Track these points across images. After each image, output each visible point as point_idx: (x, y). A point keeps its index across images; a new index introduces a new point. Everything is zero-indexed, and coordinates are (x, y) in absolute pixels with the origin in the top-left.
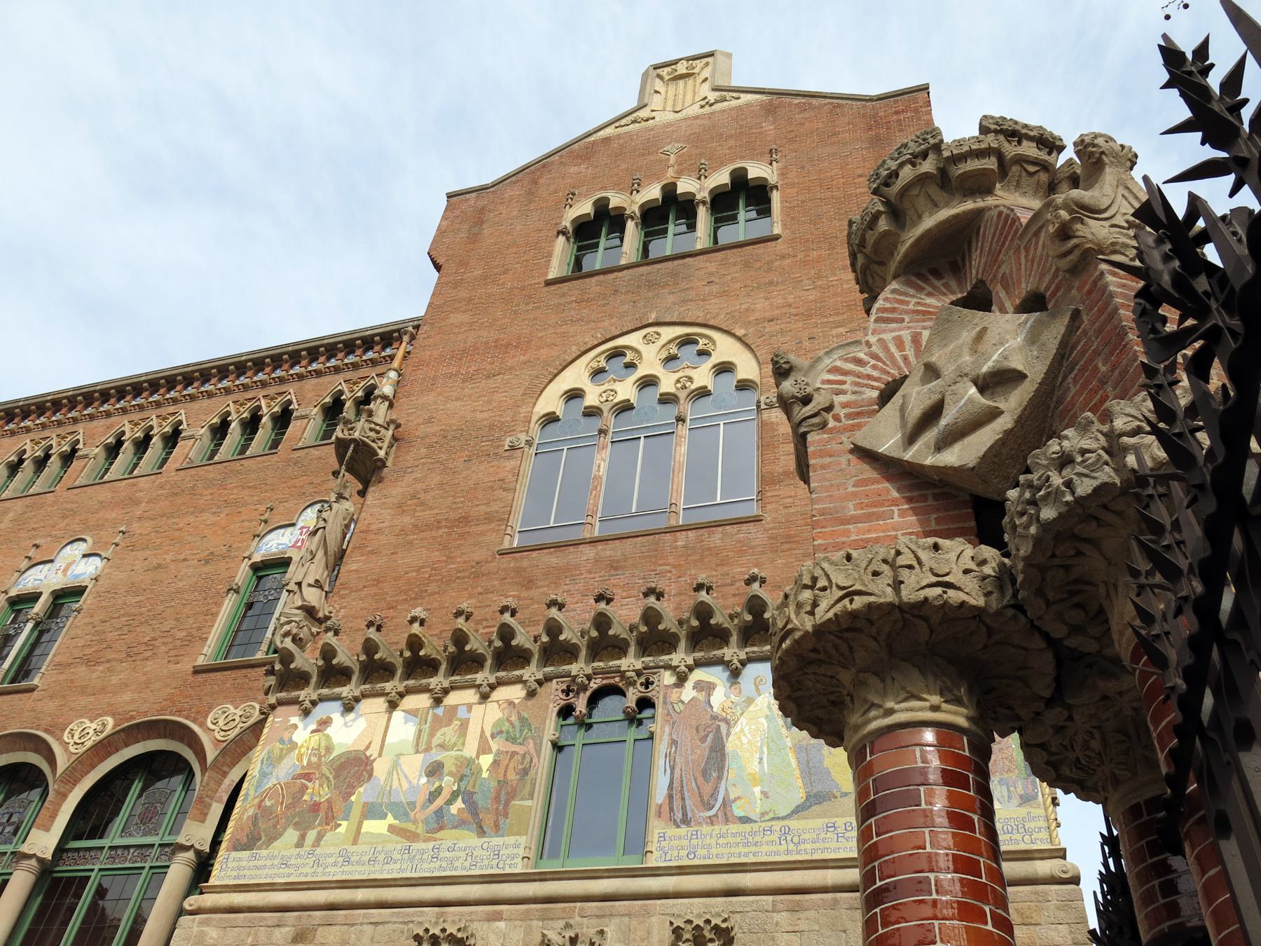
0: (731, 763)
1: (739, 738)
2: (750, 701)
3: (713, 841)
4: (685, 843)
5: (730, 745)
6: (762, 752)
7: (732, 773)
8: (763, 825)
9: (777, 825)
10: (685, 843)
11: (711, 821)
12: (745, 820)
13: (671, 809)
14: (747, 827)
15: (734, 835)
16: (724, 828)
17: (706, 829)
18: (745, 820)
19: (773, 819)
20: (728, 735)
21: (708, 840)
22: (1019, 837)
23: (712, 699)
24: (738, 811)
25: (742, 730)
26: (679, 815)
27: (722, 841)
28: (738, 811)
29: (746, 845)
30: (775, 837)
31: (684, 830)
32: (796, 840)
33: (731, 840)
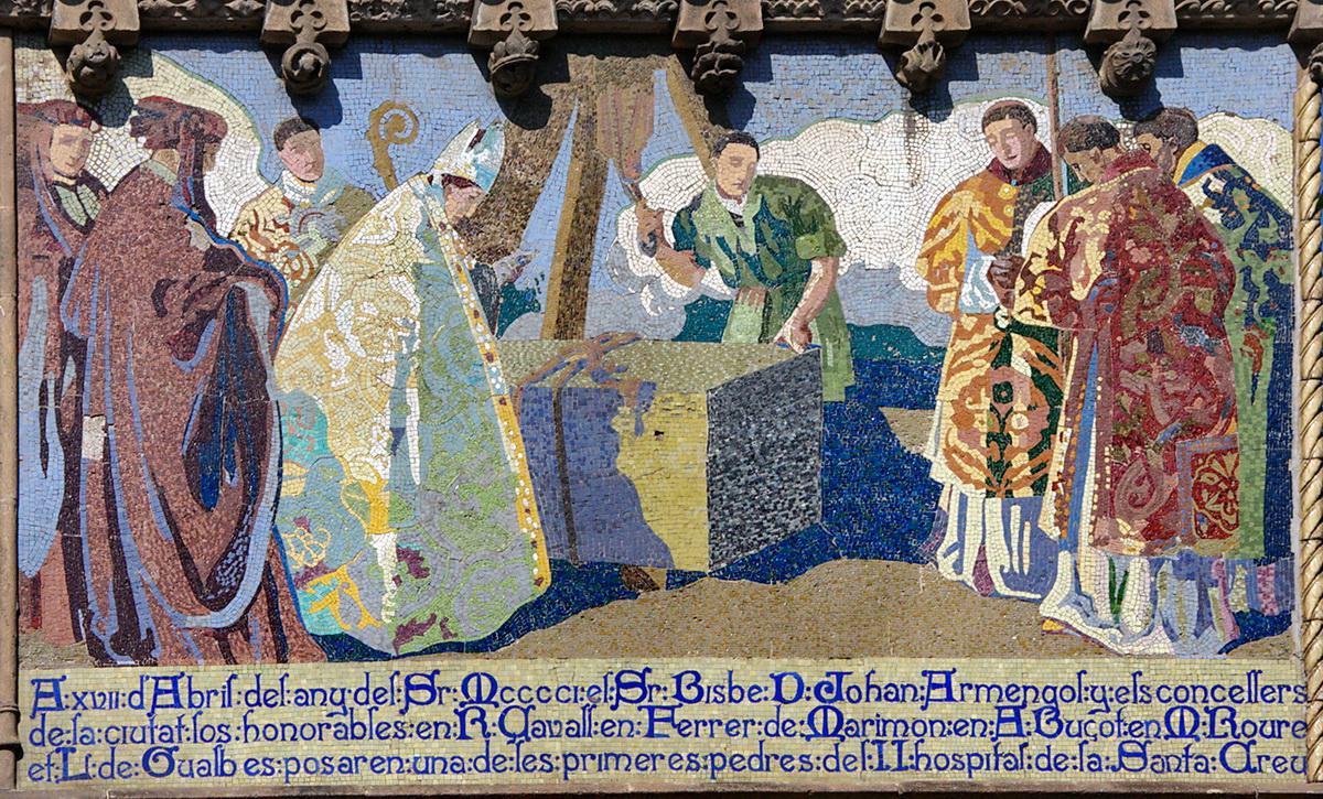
0: (292, 443)
1: (318, 350)
2: (354, 204)
3: (233, 716)
4: (139, 718)
5: (286, 374)
6: (399, 406)
7: (294, 480)
8: (406, 667)
9: (452, 671)
10: (139, 718)
11: (224, 645)
12: (343, 648)
13: (77, 598)
14: (349, 675)
15: (305, 697)
16: (271, 674)
17: (210, 675)
18: (343, 648)
19: (439, 649)
20: (278, 329)
21: (214, 714)
22: (1211, 748)
23: (212, 182)
24: (320, 611)
25: (327, 319)
26: (108, 627)
27: (261, 716)
28: (320, 611)
29: (348, 733)
30: (445, 711)
31: (124, 676)
32: (515, 723)
33: (290, 713)
